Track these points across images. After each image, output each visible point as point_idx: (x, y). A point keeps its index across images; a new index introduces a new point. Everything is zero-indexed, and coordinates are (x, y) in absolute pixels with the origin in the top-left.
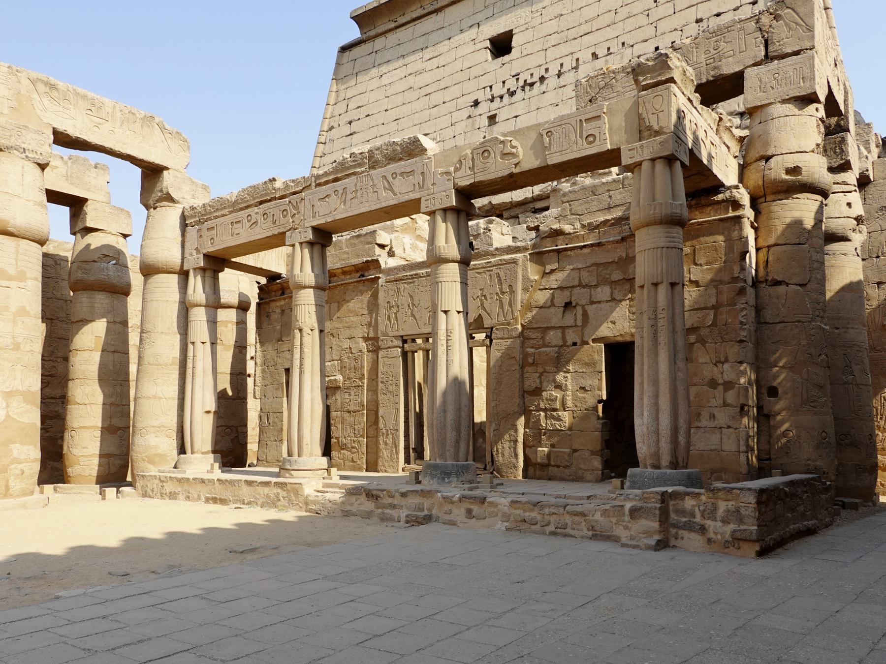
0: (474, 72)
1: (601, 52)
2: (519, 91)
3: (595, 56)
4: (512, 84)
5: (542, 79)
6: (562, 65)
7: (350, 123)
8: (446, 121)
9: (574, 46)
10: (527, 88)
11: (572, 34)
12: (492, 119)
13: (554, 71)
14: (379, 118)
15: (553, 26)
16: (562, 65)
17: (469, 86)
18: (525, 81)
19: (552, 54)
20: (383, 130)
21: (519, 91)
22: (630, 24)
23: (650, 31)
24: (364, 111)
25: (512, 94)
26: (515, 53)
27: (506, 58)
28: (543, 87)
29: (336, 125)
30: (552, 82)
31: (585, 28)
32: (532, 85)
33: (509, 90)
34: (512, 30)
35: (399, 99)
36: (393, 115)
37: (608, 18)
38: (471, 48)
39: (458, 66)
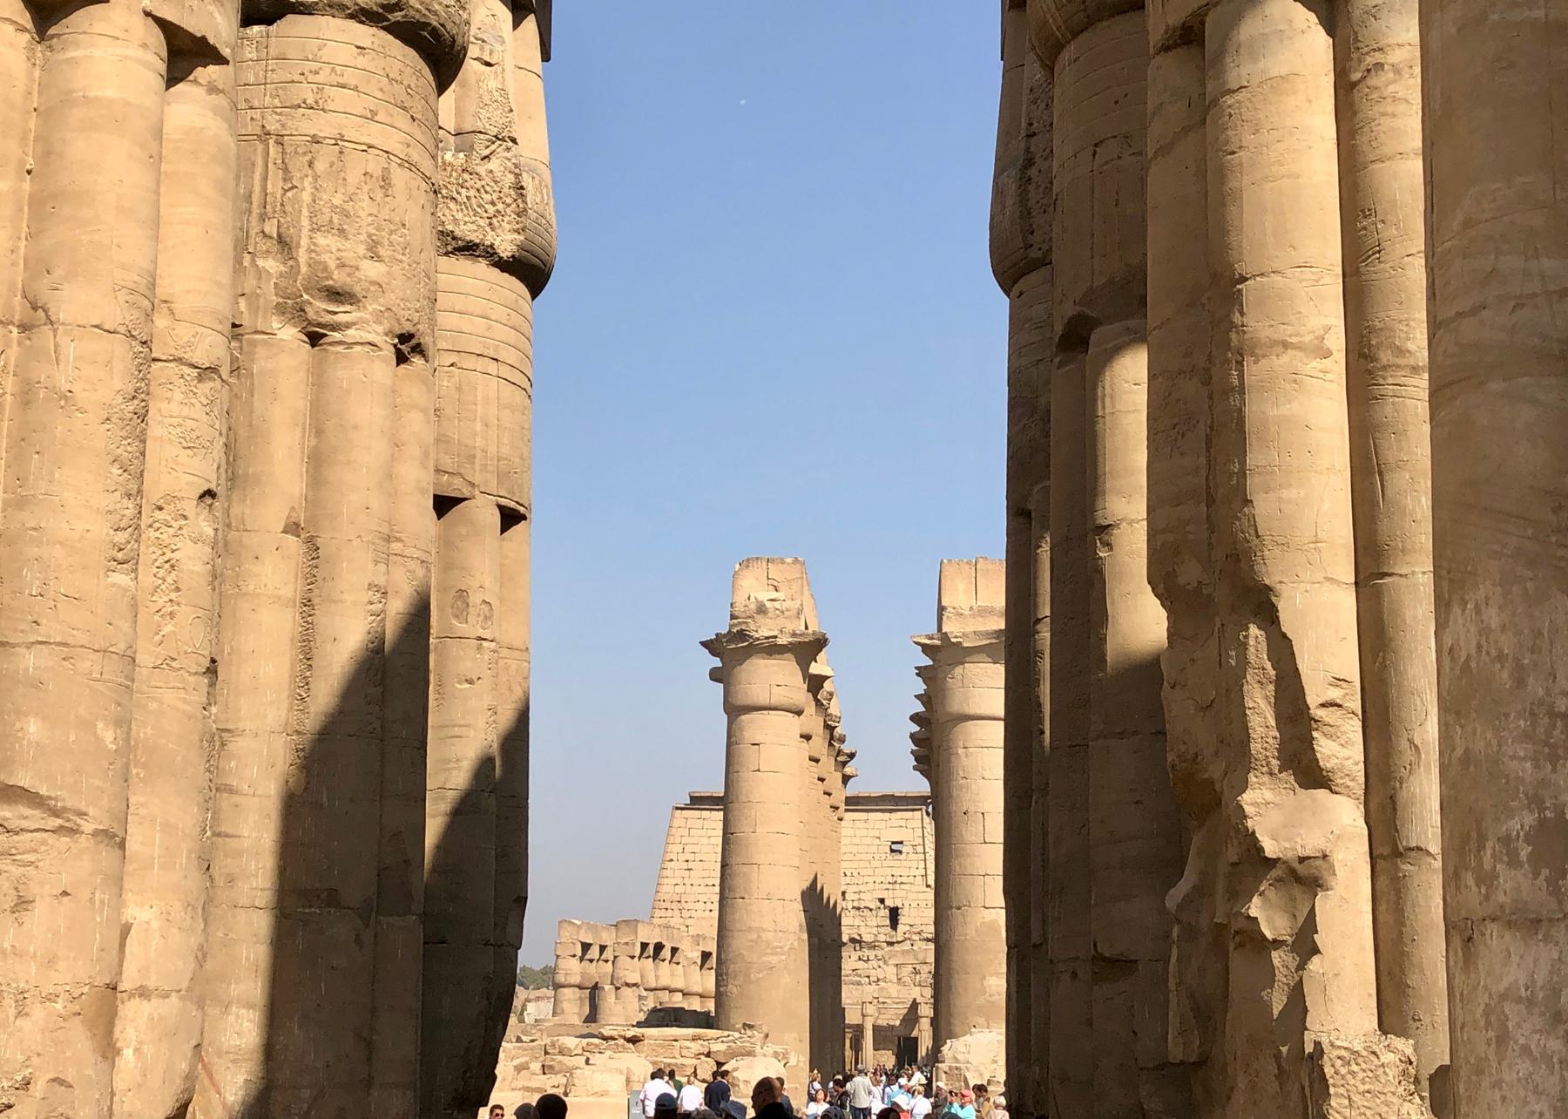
22: (862, 864)
24: (698, 857)
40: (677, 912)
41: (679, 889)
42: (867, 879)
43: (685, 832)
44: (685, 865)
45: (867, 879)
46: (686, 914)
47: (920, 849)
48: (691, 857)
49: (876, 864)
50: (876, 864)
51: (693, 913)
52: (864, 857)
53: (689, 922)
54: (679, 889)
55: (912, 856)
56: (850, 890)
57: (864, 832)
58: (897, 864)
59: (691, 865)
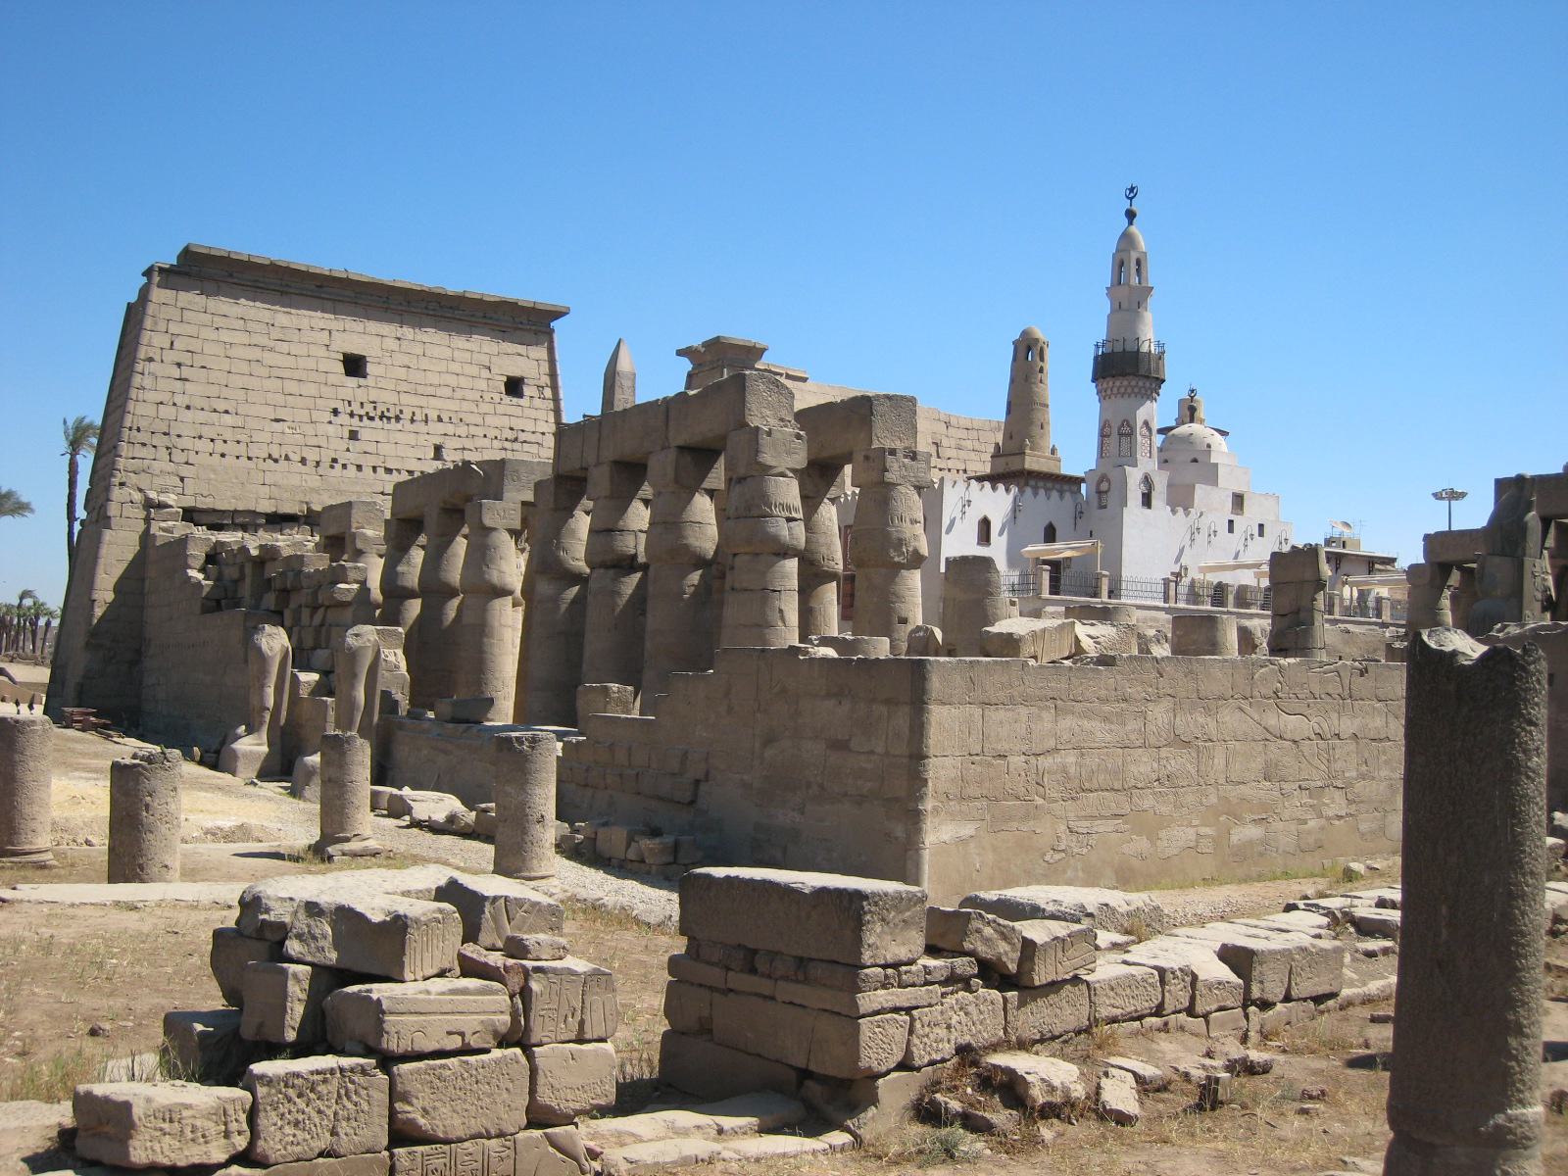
0: (332, 379)
1: (445, 418)
2: (377, 419)
3: (440, 420)
4: (369, 408)
5: (398, 419)
6: (414, 413)
7: (179, 365)
8: (304, 416)
9: (423, 401)
10: (385, 419)
11: (420, 389)
12: (353, 436)
13: (407, 415)
14: (223, 378)
15: (402, 373)
16: (414, 413)
17: (326, 391)
18: (383, 412)
19: (405, 399)
20: (225, 393)
21: (377, 419)
22: (466, 406)
23: (479, 421)
24: (199, 361)
25: (371, 419)
26: (370, 381)
27: (362, 381)
28: (399, 426)
29: (157, 358)
30: (405, 423)
31: (430, 390)
32: (389, 419)
33: (367, 413)
34: (364, 357)
35: (244, 367)
36: (237, 381)
37: (447, 392)
38: (322, 352)
39: (311, 364)
40: (163, 453)
41: (167, 412)
42: (473, 430)
43: (175, 314)
44: (176, 372)
45: (473, 430)
46: (178, 457)
47: (548, 393)
48: (186, 358)
49: (485, 408)
50: (485, 408)
51: (193, 458)
52: (470, 395)
53: (185, 471)
54: (167, 412)
55: (537, 402)
56: (450, 444)
57: (468, 355)
58: (518, 411)
59: (186, 372)
